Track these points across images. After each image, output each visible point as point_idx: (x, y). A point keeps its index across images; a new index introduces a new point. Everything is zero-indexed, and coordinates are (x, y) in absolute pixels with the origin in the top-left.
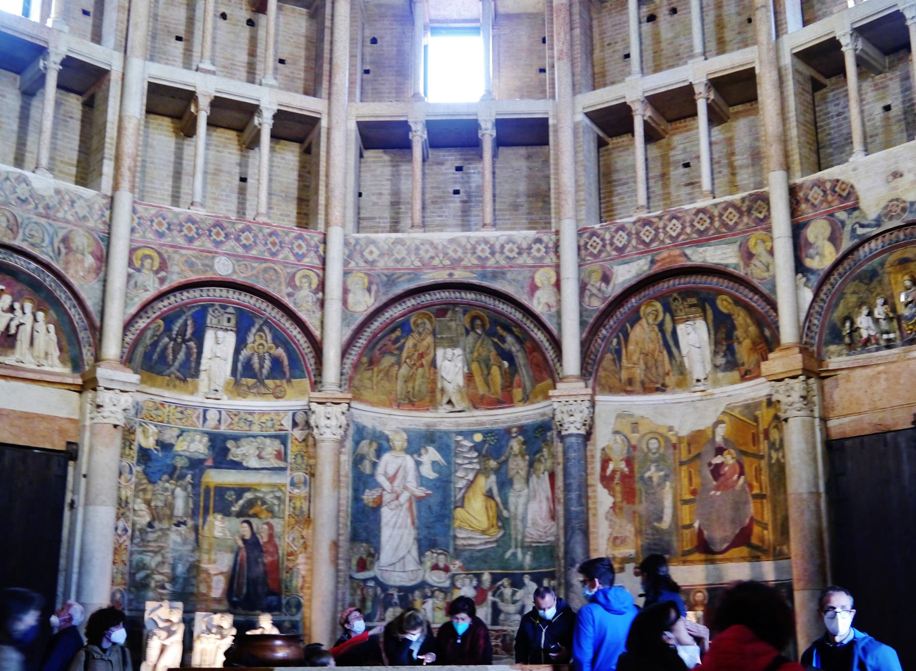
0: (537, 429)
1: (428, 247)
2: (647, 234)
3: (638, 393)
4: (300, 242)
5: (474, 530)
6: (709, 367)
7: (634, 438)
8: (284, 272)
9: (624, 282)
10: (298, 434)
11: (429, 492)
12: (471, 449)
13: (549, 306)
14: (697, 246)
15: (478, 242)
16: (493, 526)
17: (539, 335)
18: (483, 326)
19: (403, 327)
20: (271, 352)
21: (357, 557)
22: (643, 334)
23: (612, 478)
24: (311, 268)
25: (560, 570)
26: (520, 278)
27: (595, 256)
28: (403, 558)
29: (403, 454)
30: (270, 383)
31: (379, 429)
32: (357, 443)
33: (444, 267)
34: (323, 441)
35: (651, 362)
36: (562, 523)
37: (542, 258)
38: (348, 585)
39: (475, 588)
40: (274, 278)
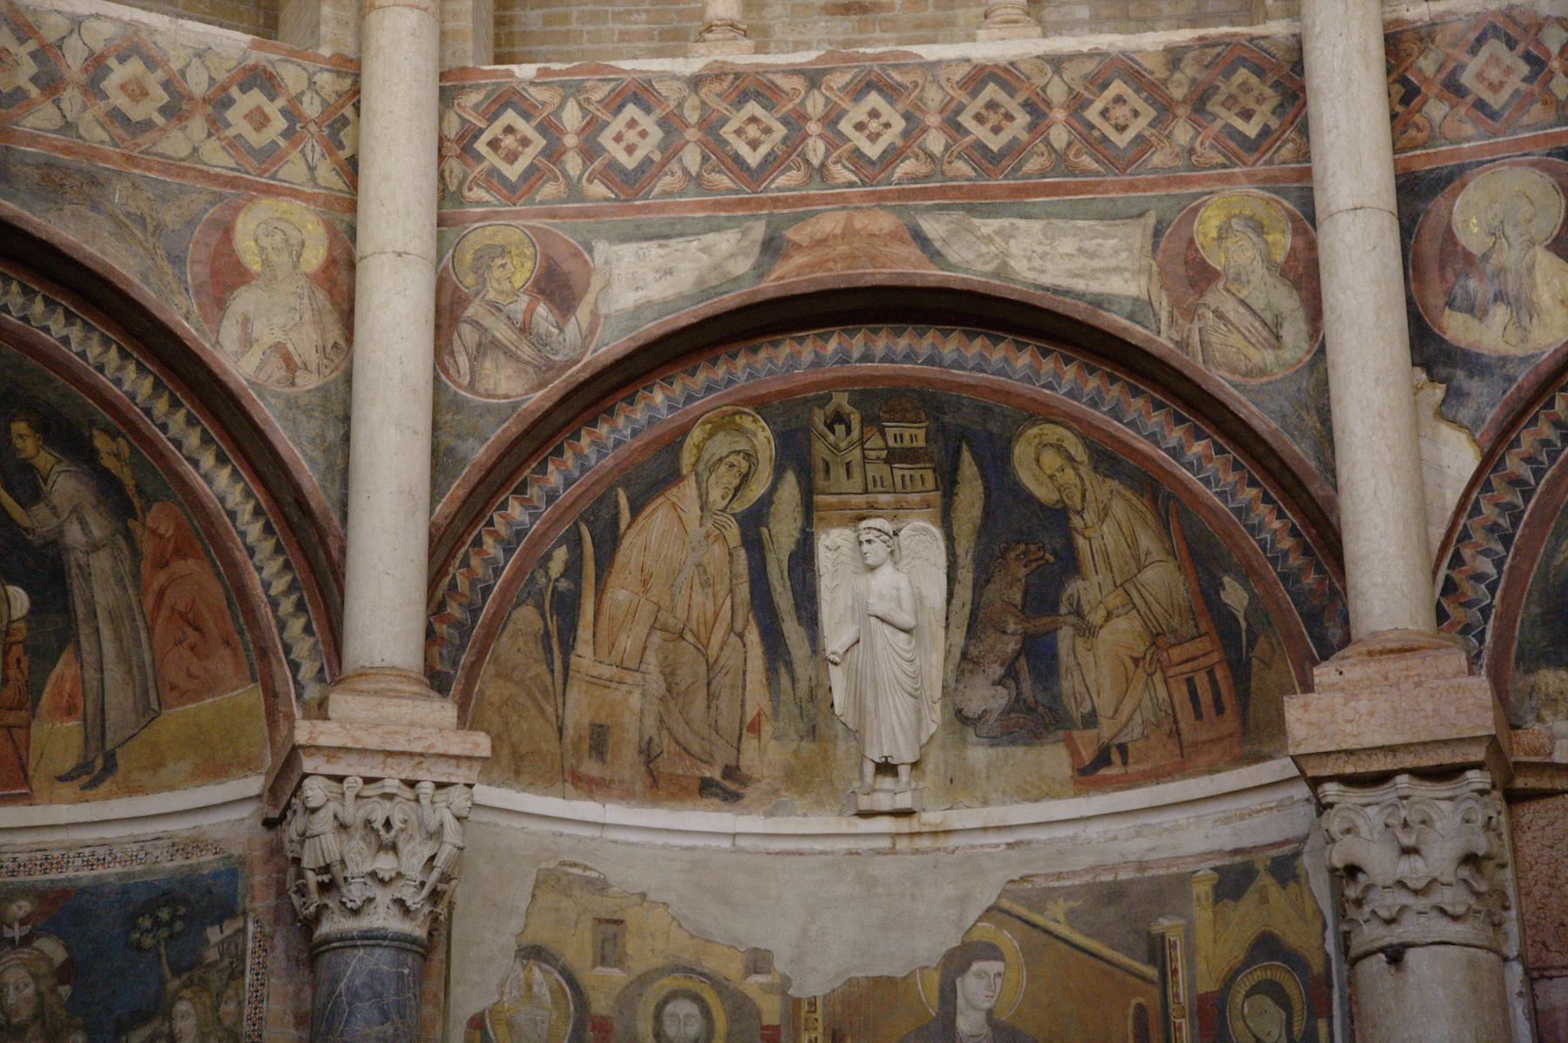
0: (150, 907)
2: (751, 134)
3: (627, 795)
6: (934, 720)
7: (604, 985)
14: (971, 210)
17: (223, 486)
22: (678, 546)
26: (169, 216)
27: (511, 191)
35: (691, 671)
37: (270, 156)
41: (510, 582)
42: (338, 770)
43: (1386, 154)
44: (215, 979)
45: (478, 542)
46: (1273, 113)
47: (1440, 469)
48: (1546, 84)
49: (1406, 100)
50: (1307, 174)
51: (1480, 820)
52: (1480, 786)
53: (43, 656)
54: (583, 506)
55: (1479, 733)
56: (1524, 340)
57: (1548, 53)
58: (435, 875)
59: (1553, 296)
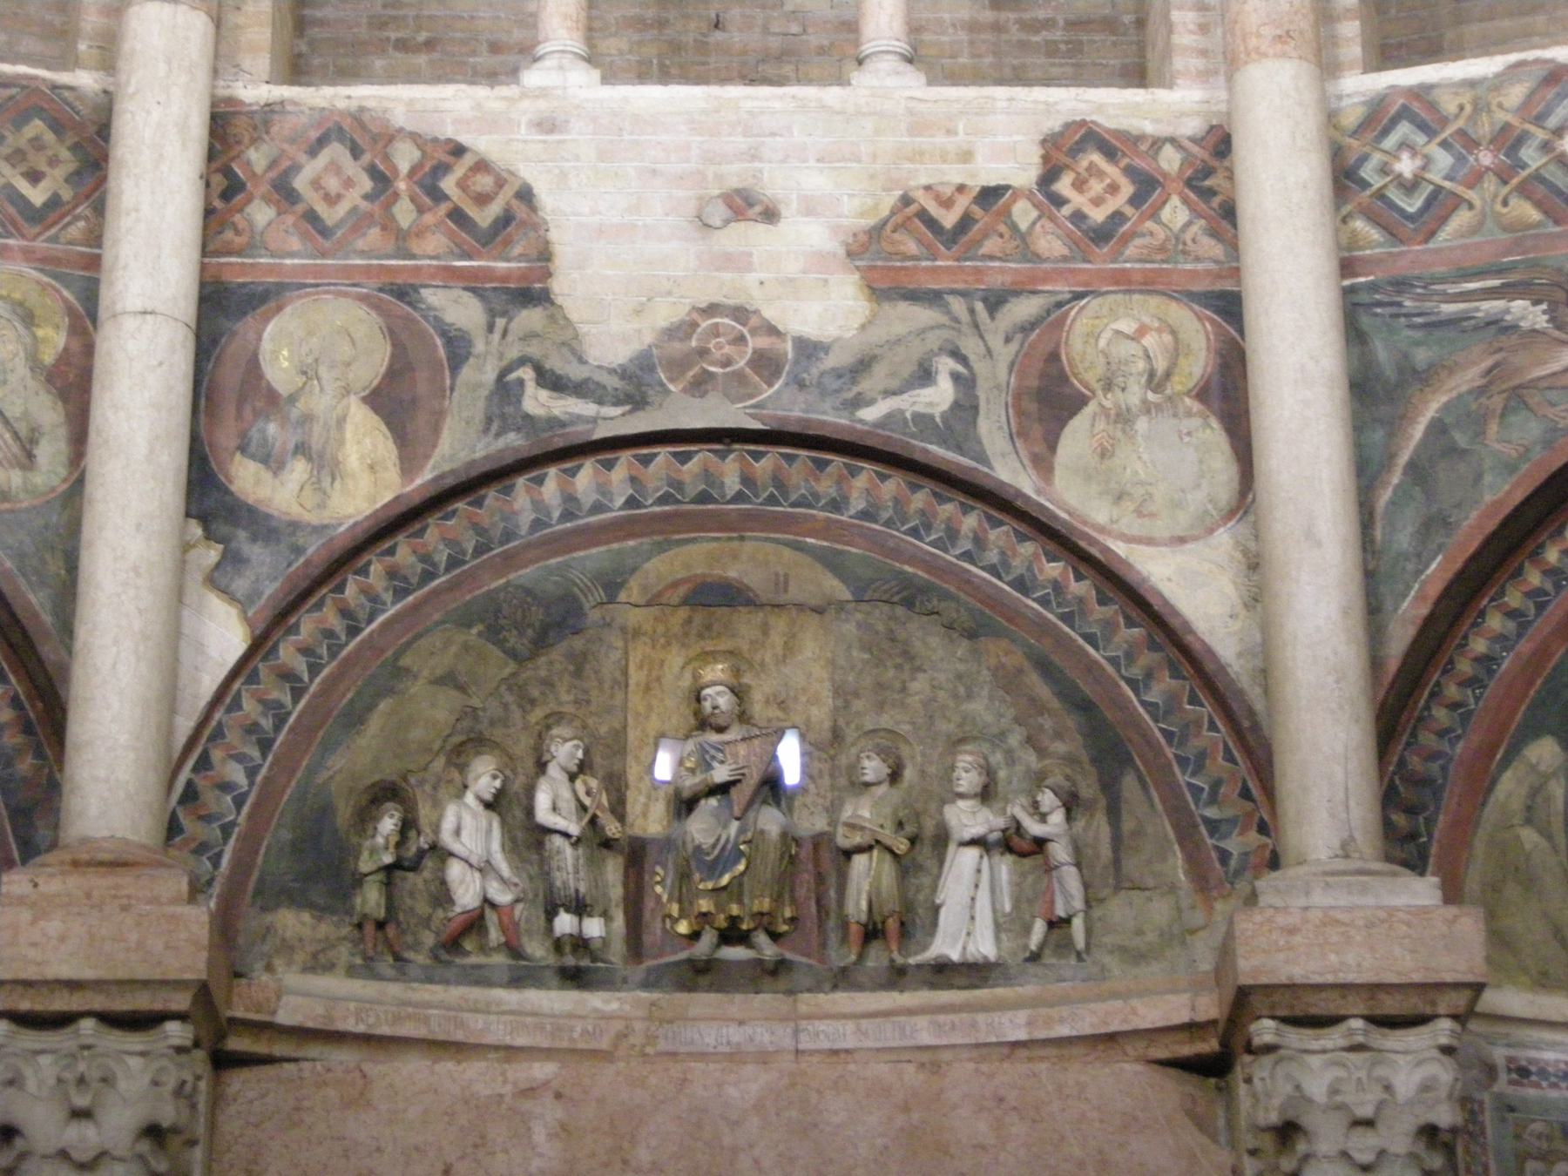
43: (191, 253)
46: (67, 181)
47: (200, 647)
48: (388, 206)
49: (226, 195)
50: (94, 262)
51: (171, 1082)
52: (177, 1042)
55: (188, 976)
56: (322, 506)
57: (395, 171)
59: (362, 458)
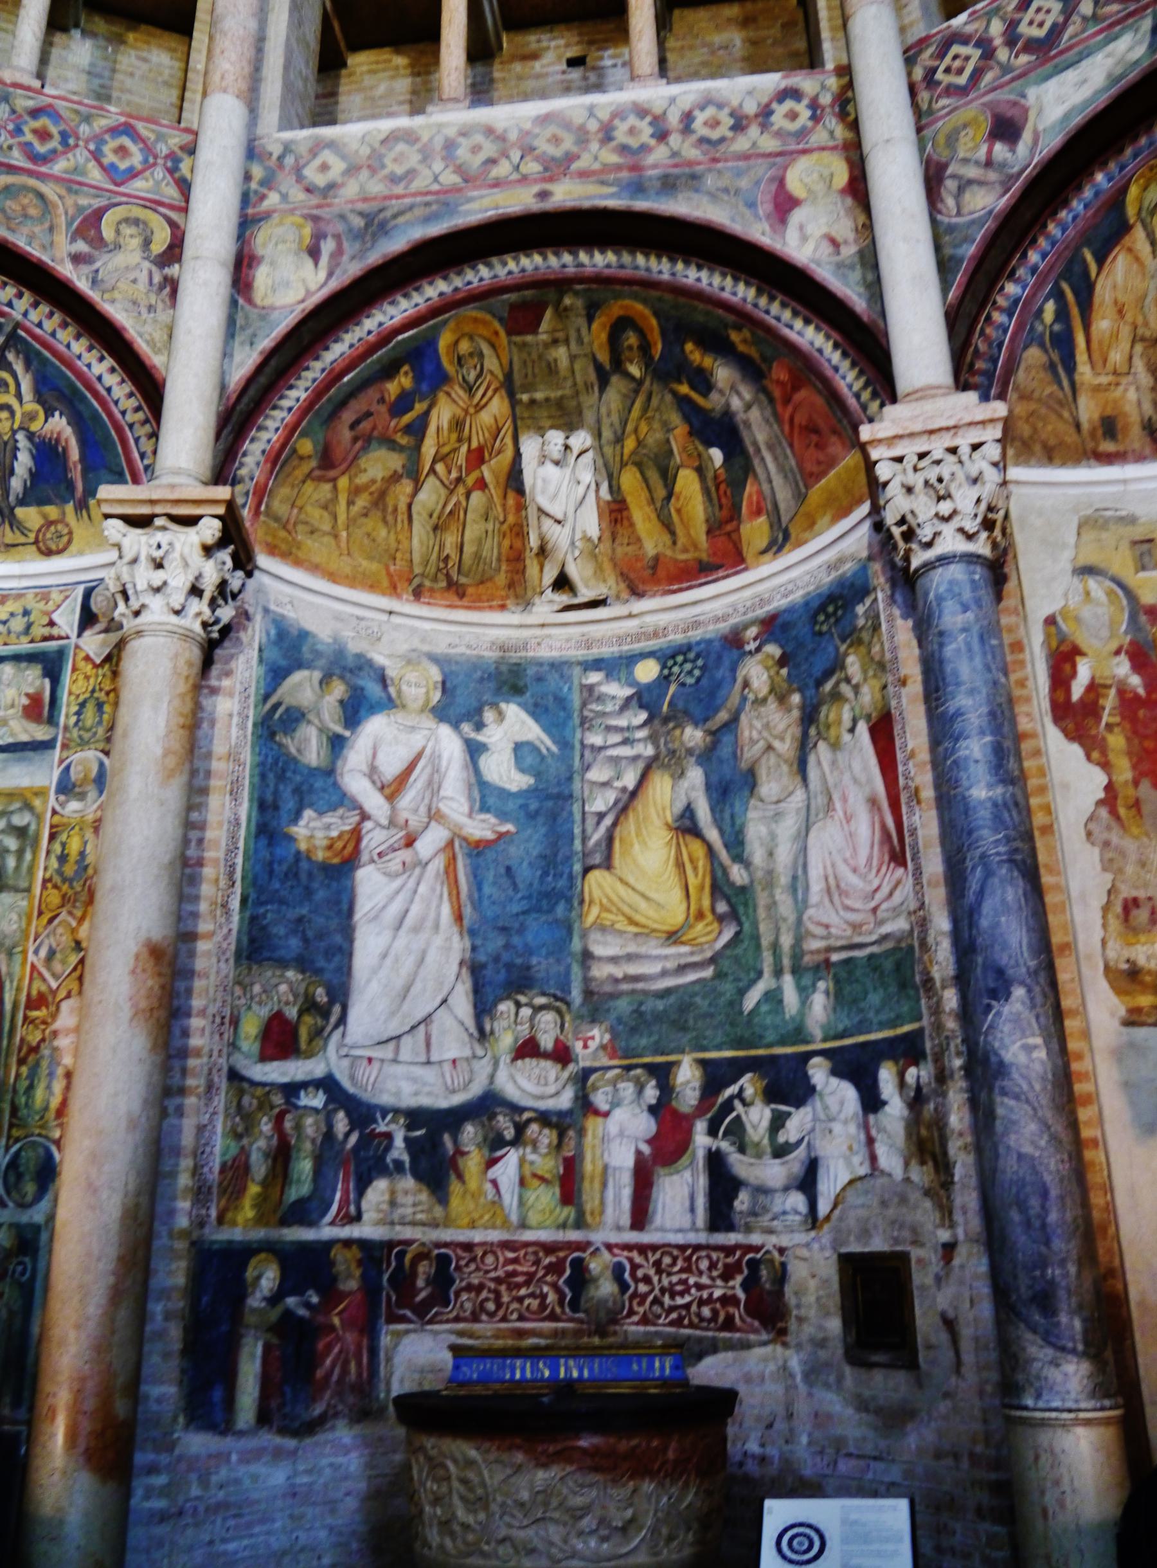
0: (822, 608)
1: (479, 138)
3: (1140, 458)
4: (125, 141)
5: (644, 933)
8: (66, 207)
9: (1067, 116)
10: (94, 643)
11: (509, 827)
12: (627, 703)
13: (835, 243)
15: (618, 114)
16: (700, 915)
17: (809, 336)
18: (645, 348)
19: (416, 358)
20: (35, 427)
21: (265, 1012)
23: (1090, 706)
24: (154, 204)
25: (938, 1027)
26: (744, 183)
27: (962, 91)
28: (427, 1020)
29: (428, 722)
30: (30, 515)
31: (354, 646)
32: (277, 675)
33: (524, 179)
34: (139, 633)
36: (934, 864)
37: (802, 134)
38: (220, 1101)
39: (653, 1110)
40: (32, 212)
41: (1015, 334)
42: (897, 452)
44: (865, 636)
45: (989, 318)
53: (738, 485)
54: (1058, 269)
58: (983, 506)
